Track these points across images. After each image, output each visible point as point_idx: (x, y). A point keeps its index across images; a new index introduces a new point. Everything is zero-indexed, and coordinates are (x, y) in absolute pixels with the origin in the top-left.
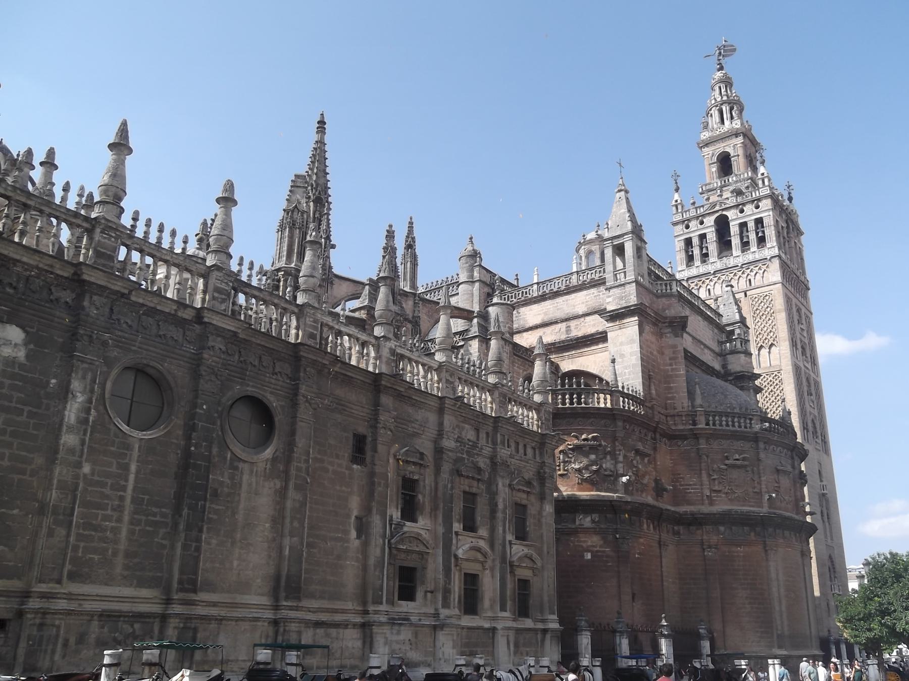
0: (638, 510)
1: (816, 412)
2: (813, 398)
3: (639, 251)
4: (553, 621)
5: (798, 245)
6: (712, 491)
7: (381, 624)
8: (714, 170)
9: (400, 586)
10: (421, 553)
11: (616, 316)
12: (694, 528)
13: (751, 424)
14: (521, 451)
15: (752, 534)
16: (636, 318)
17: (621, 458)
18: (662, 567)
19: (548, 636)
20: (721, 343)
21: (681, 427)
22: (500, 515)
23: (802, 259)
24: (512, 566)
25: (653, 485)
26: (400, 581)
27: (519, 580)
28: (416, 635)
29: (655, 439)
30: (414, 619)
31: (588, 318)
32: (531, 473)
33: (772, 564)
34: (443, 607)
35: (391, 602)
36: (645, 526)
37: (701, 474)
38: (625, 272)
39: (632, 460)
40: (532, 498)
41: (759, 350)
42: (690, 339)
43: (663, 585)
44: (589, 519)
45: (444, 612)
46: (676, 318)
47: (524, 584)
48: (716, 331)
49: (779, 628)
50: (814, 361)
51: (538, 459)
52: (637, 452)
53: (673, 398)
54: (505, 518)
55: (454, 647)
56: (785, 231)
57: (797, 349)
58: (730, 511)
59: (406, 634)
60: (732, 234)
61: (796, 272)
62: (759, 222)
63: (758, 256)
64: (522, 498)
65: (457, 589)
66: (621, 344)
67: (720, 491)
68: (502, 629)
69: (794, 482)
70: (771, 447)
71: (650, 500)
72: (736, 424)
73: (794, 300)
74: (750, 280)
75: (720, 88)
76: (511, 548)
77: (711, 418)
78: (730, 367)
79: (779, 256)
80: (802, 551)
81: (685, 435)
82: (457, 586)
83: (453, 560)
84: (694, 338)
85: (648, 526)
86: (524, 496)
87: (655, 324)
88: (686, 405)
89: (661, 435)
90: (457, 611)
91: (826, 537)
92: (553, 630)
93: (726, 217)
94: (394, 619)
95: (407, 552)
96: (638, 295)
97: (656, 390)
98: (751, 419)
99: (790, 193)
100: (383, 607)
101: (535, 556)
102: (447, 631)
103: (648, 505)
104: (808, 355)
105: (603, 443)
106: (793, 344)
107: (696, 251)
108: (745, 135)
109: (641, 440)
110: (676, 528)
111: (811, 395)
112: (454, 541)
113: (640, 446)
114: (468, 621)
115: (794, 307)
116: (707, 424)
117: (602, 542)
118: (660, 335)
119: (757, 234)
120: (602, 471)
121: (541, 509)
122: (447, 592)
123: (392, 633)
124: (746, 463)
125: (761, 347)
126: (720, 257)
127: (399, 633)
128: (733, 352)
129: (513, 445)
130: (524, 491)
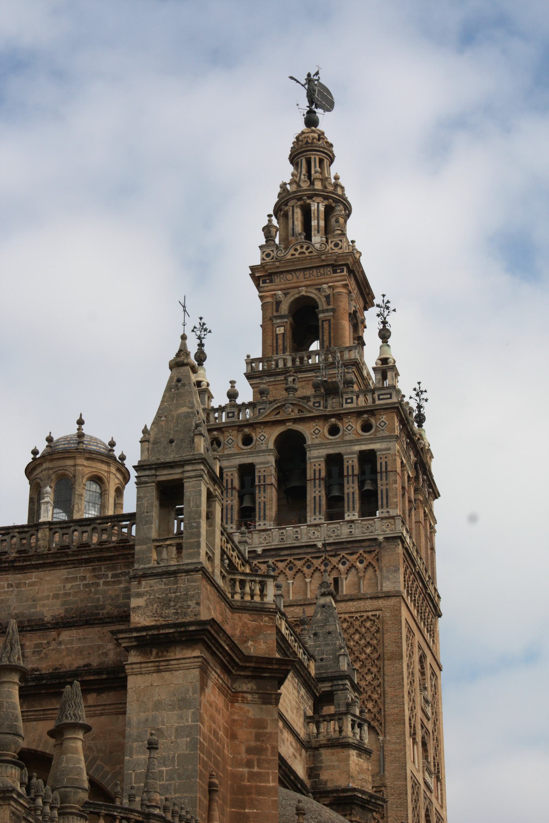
23: (433, 549)
31: (66, 635)
38: (179, 547)
63: (358, 533)
78: (324, 776)
93: (300, 438)
108: (351, 272)
118: (232, 696)
119: (361, 484)
126: (281, 521)
128: (339, 744)
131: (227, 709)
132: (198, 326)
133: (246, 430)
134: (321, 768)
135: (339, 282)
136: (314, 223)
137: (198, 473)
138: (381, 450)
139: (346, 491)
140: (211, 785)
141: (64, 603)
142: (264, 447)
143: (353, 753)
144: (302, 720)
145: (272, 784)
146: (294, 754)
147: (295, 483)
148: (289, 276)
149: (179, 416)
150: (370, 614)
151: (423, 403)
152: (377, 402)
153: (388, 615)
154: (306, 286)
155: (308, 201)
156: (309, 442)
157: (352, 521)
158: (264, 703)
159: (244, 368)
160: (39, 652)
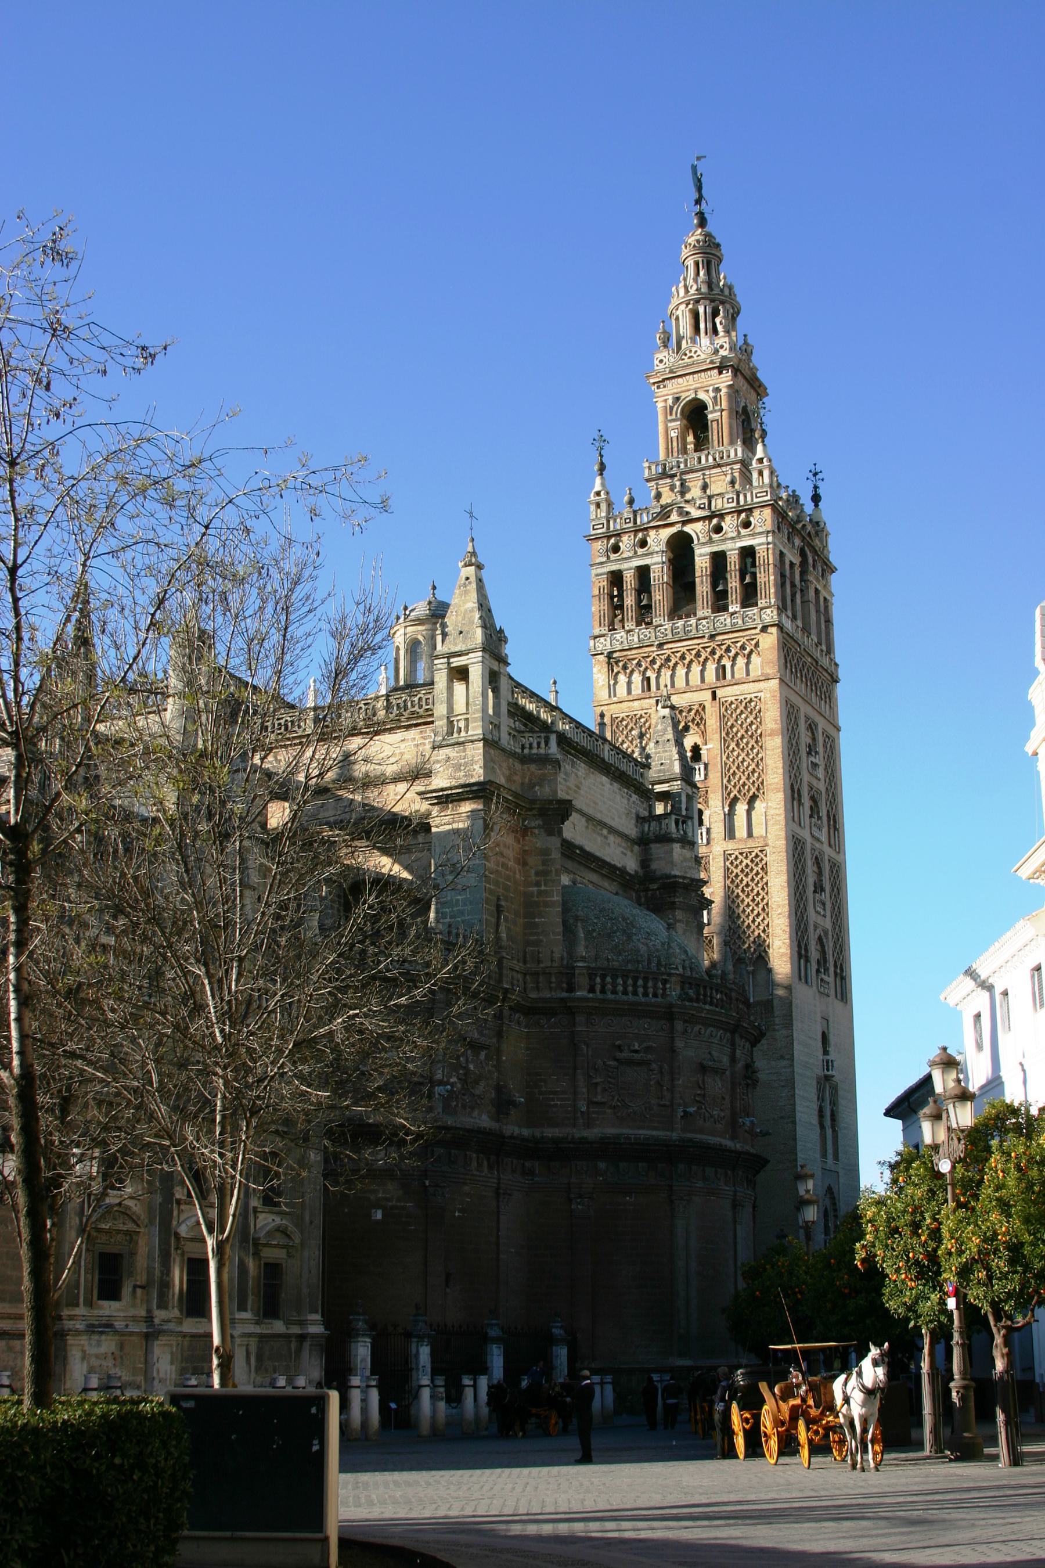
1: (828, 924)
2: (826, 896)
3: (493, 679)
4: (314, 1322)
5: (823, 593)
6: (591, 1103)
7: (78, 1333)
8: (673, 434)
9: (100, 1280)
10: (128, 1233)
13: (664, 989)
18: (498, 1230)
19: (307, 1345)
20: (640, 820)
21: (547, 994)
23: (828, 621)
25: (493, 1095)
26: (100, 1274)
27: (266, 1264)
28: (121, 1346)
30: (119, 1325)
34: (159, 1307)
35: (89, 1304)
36: (474, 1164)
42: (584, 820)
45: (160, 1315)
46: (550, 802)
47: (272, 1271)
48: (635, 797)
50: (835, 824)
53: (538, 943)
55: (172, 1363)
57: (800, 803)
59: (108, 1345)
60: (698, 574)
62: (748, 553)
67: (604, 1103)
70: (696, 1028)
71: (484, 1120)
72: (641, 990)
75: (697, 264)
76: (256, 1218)
77: (598, 980)
78: (654, 866)
79: (780, 626)
80: (734, 1200)
84: (590, 819)
85: (480, 1165)
88: (557, 956)
90: (176, 1313)
91: (824, 1155)
92: (314, 1336)
93: (688, 538)
94: (93, 1326)
95: (108, 1232)
97: (508, 929)
98: (664, 982)
99: (816, 487)
100: (81, 1310)
101: (291, 1228)
102: (163, 1340)
103: (480, 1131)
106: (793, 794)
108: (736, 371)
110: (528, 1164)
111: (823, 890)
112: (175, 1213)
119: (742, 578)
122: (165, 1285)
123: (91, 1345)
124: (649, 1057)
125: (735, 800)
127: (99, 1344)
131: (519, 842)
134: (651, 860)
136: (702, 326)
139: (730, 585)
142: (657, 549)
143: (677, 846)
144: (633, 822)
145: (555, 898)
146: (623, 853)
149: (466, 611)
150: (753, 696)
151: (820, 484)
152: (755, 500)
153: (768, 695)
156: (696, 542)
157: (736, 613)
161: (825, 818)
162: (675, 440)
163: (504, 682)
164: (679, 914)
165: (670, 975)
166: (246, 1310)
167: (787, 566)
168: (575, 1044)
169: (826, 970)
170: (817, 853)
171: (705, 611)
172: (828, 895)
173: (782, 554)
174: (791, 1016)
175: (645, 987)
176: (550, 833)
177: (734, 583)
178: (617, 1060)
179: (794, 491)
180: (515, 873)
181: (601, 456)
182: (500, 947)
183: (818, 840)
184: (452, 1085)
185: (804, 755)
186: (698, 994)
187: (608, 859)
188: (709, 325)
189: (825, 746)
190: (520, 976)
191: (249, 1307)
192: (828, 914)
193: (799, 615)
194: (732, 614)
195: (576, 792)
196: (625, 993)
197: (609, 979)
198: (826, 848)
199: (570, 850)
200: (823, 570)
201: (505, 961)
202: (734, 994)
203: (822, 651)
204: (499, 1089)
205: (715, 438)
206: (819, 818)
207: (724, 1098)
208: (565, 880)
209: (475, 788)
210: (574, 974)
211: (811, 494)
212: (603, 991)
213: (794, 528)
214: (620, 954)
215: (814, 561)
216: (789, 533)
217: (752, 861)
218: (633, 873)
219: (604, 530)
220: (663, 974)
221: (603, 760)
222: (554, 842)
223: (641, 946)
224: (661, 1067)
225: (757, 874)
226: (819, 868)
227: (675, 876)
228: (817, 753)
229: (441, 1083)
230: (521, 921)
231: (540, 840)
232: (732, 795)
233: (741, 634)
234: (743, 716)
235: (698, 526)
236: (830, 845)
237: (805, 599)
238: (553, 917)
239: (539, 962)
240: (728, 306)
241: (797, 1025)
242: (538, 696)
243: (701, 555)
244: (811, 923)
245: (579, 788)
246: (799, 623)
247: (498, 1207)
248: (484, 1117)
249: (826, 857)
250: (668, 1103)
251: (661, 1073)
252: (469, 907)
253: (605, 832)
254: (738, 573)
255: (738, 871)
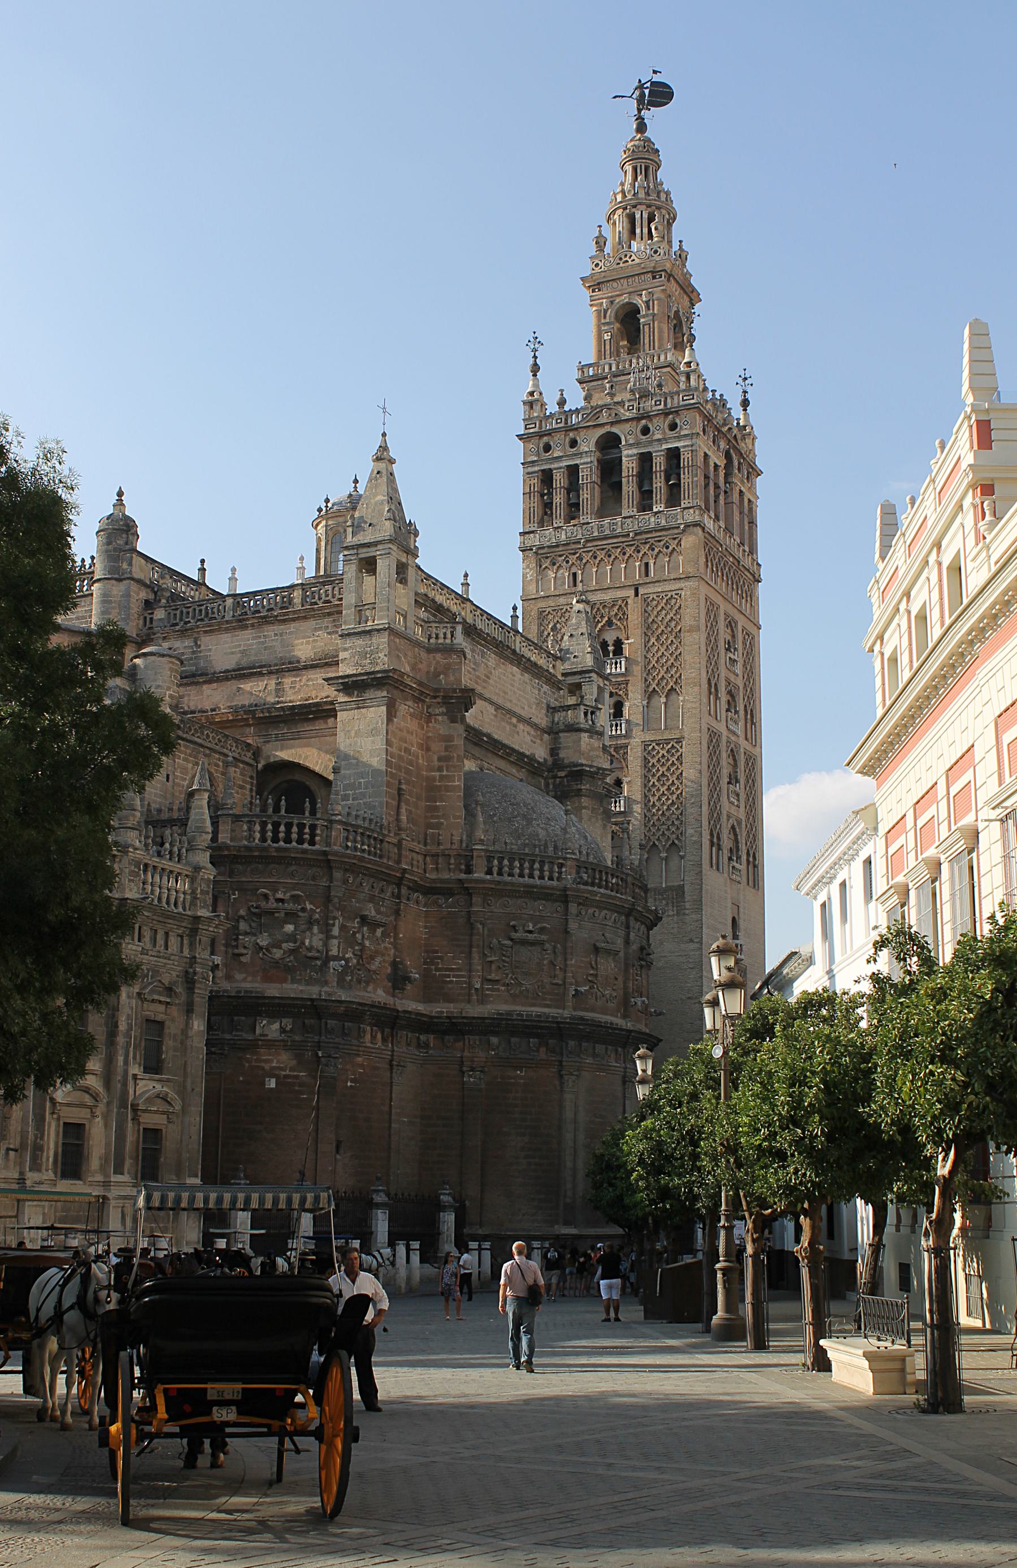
0: (355, 1014)
1: (742, 814)
2: (740, 788)
5: (747, 495)
8: (607, 337)
11: (355, 686)
12: (451, 1038)
13: (560, 873)
14: (160, 941)
15: (543, 1049)
16: (385, 694)
17: (336, 931)
18: (391, 1100)
20: (552, 710)
22: (121, 1040)
23: (752, 523)
24: (135, 1109)
25: (389, 971)
29: (399, 897)
32: (174, 974)
33: (568, 1097)
34: (30, 1170)
36: (368, 1037)
37: (470, 952)
39: (354, 933)
40: (174, 1011)
41: (649, 698)
42: (491, 709)
43: (390, 1127)
44: (276, 1026)
45: (31, 1177)
46: (454, 691)
47: (153, 1135)
48: (546, 688)
49: (569, 1193)
50: (752, 718)
51: (186, 952)
52: (364, 920)
54: (128, 1044)
56: (722, 473)
57: (717, 698)
58: (509, 1013)
61: (735, 551)
62: (674, 455)
64: (157, 1012)
65: (52, 1146)
66: (358, 733)
68: (115, 1198)
69: (626, 965)
70: (591, 911)
71: (379, 995)
72: (537, 873)
73: (724, 606)
74: (647, 564)
75: (635, 169)
76: (136, 1085)
77: (496, 862)
78: (562, 754)
80: (624, 1077)
81: (451, 889)
82: (52, 1140)
83: (48, 1104)
84: (498, 707)
85: (373, 1037)
86: (162, 1008)
87: (417, 700)
88: (456, 838)
89: (409, 888)
90: (51, 1175)
96: (393, 652)
99: (745, 392)
101: (172, 1095)
104: (741, 708)
105: (309, 906)
106: (713, 689)
107: (559, 499)
109: (372, 899)
111: (737, 781)
113: (370, 911)
114: (64, 1186)
115: (721, 618)
116: (489, 872)
117: (294, 1062)
119: (667, 480)
120: (303, 951)
121: (187, 1025)
122: (38, 1149)
124: (544, 937)
126: (601, 514)
128: (573, 728)
129: (147, 934)
130: (160, 1002)
132: (532, 340)
133: (571, 435)
135: (659, 288)
136: (638, 231)
137: (387, 551)
138: (684, 447)
140: (399, 789)
141: (314, 647)
144: (544, 711)
147: (615, 479)
148: (615, 284)
149: (376, 503)
151: (749, 389)
152: (681, 403)
153: (688, 593)
154: (630, 293)
155: (633, 210)
156: (623, 443)
157: (660, 512)
158: (452, 722)
159: (577, 375)
160: (294, 688)
161: (742, 713)
162: (608, 343)
163: (411, 572)
164: (585, 801)
165: (565, 859)
166: (122, 1174)
167: (712, 469)
168: (472, 924)
169: (739, 858)
170: (732, 746)
171: (631, 510)
172: (743, 786)
173: (706, 455)
174: (701, 901)
175: (541, 870)
176: (453, 720)
177: (659, 483)
178: (512, 940)
179: (721, 395)
180: (418, 758)
181: (535, 357)
182: (400, 829)
183: (734, 733)
184: (347, 961)
185: (723, 651)
186: (594, 878)
187: (517, 747)
188: (645, 230)
189: (744, 643)
190: (420, 858)
191: (126, 1171)
192: (742, 805)
193: (722, 516)
194: (656, 513)
195: (484, 681)
196: (521, 875)
197: (506, 862)
198: (742, 741)
199: (476, 738)
200: (748, 473)
201: (404, 842)
202: (629, 879)
203: (744, 551)
204: (394, 964)
205: (647, 341)
206: (736, 712)
207: (616, 979)
208: (470, 765)
209: (379, 675)
210: (472, 857)
211: (740, 398)
212: (500, 873)
213: (719, 431)
214: (519, 838)
215: (739, 463)
216: (714, 435)
217: (668, 752)
218: (541, 760)
219: (536, 430)
220: (559, 858)
221: (514, 651)
222: (460, 729)
223: (540, 831)
224: (555, 947)
225: (673, 764)
226: (735, 760)
227: (582, 765)
228: (735, 649)
229: (336, 958)
230: (423, 804)
231: (441, 726)
232: (651, 689)
233: (664, 533)
234: (664, 612)
235: (627, 427)
236: (746, 739)
237: (729, 500)
238: (454, 802)
239: (439, 844)
240: (664, 212)
241: (706, 910)
242: (448, 588)
243: (628, 456)
244: (724, 813)
245: (489, 678)
246: (722, 524)
247: (391, 1077)
248: (380, 992)
249: (742, 750)
250: (560, 982)
251: (554, 952)
252: (371, 790)
253: (514, 720)
254: (662, 474)
255: (655, 761)
